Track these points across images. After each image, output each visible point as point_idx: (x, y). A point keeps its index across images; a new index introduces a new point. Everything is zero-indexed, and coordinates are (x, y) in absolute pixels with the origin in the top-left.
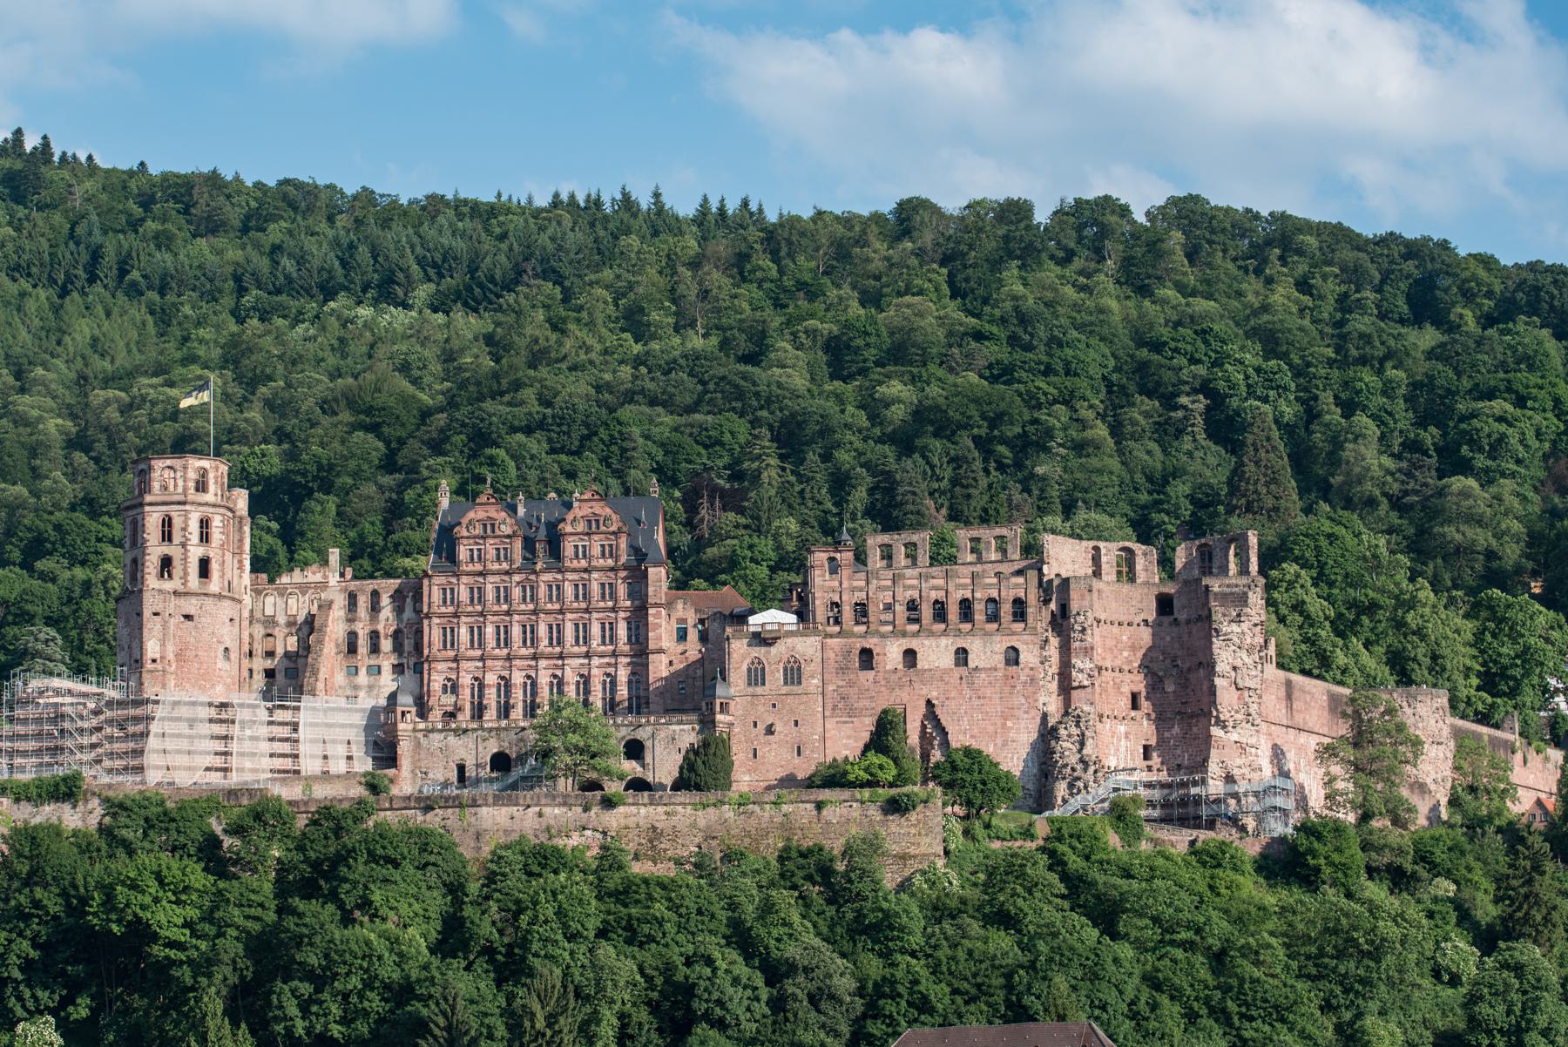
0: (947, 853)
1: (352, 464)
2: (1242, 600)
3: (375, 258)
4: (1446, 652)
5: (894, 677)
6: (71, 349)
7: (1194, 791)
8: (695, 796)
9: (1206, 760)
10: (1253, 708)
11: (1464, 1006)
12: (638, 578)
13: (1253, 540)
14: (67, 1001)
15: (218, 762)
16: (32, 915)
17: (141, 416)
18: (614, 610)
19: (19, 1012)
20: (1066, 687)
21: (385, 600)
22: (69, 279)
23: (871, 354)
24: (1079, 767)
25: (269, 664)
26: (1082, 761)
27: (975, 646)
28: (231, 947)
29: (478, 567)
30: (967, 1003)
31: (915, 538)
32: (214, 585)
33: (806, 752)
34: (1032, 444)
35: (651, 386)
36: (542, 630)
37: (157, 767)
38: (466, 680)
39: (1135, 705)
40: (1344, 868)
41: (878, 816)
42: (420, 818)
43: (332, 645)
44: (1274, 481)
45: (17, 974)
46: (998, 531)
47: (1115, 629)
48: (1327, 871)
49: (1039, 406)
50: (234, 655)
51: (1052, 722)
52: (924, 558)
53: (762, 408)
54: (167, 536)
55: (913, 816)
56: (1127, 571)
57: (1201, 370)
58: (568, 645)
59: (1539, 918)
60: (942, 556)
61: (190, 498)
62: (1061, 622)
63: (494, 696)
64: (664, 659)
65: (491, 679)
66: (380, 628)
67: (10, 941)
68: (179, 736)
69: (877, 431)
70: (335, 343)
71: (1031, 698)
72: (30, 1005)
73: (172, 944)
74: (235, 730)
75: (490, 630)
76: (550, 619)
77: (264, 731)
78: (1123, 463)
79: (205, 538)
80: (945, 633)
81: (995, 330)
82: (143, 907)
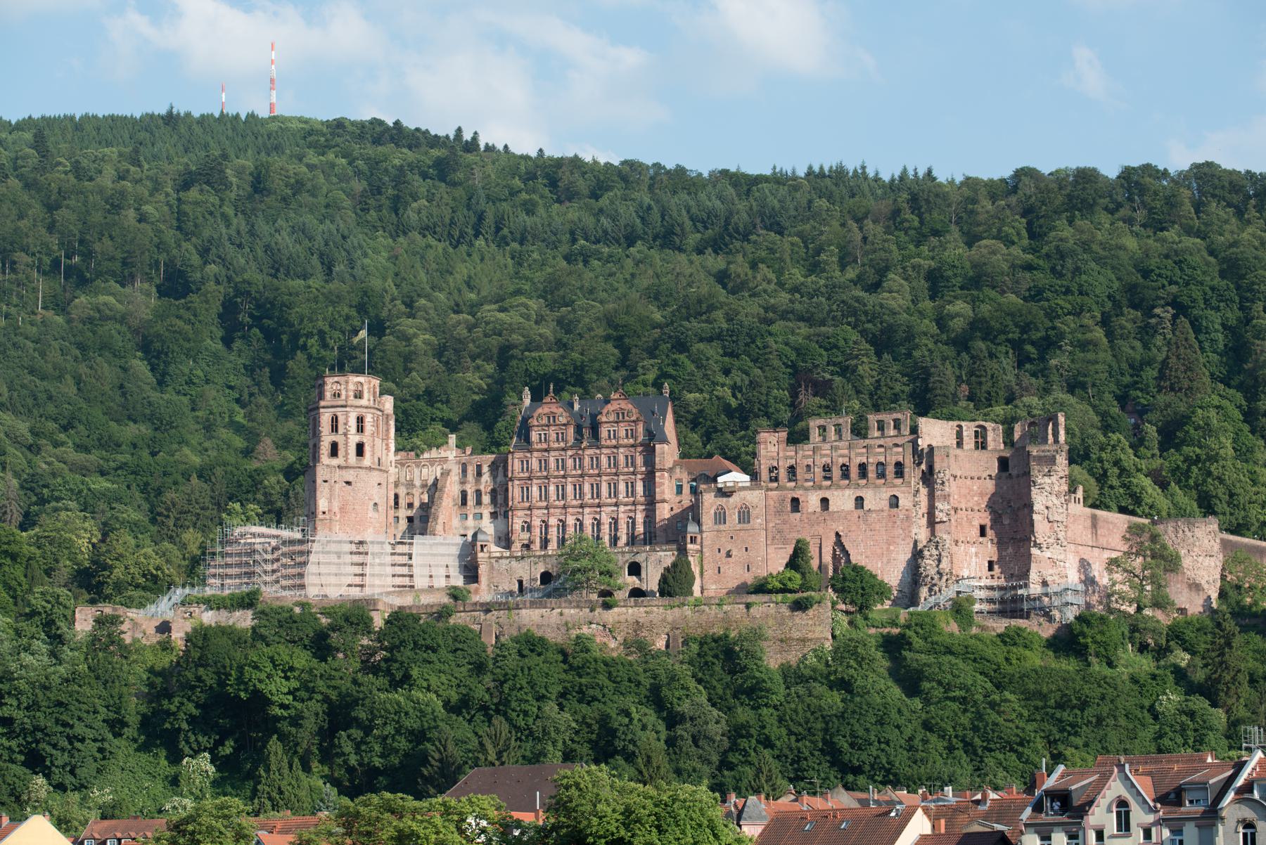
0: (834, 637)
1: (597, 365)
2: (1052, 461)
3: (663, 219)
4: (1238, 491)
5: (814, 517)
6: (452, 285)
7: (1020, 592)
8: (666, 600)
9: (1028, 571)
10: (1061, 535)
11: (1155, 739)
12: (649, 453)
13: (1061, 419)
14: (220, 742)
15: (358, 580)
16: (195, 687)
17: (478, 332)
18: (634, 473)
19: (187, 750)
20: (932, 523)
21: (485, 469)
22: (462, 236)
23: (958, 281)
24: (936, 577)
25: (410, 513)
26: (939, 573)
28: (315, 706)
29: (545, 446)
30: (798, 741)
31: (841, 421)
32: (367, 460)
33: (753, 569)
34: (1049, 344)
35: (797, 306)
36: (587, 488)
37: (315, 585)
38: (537, 522)
40: (1105, 645)
41: (787, 613)
42: (483, 617)
43: (450, 500)
44: (1189, 369)
45: (185, 726)
46: (895, 416)
47: (969, 482)
48: (1092, 648)
49: (1058, 317)
50: (381, 508)
51: (920, 546)
52: (847, 434)
53: (869, 321)
54: (335, 429)
55: (810, 612)
56: (981, 445)
57: (1174, 289)
58: (603, 498)
59: (1228, 678)
60: (859, 431)
61: (349, 403)
62: (928, 478)
63: (555, 533)
64: (667, 506)
65: (553, 521)
66: (482, 488)
67: (182, 704)
68: (329, 563)
69: (944, 337)
70: (628, 277)
71: (906, 530)
72: (195, 746)
73: (283, 706)
74: (369, 559)
75: (552, 488)
76: (592, 480)
77: (389, 559)
78: (1114, 356)
79: (360, 429)
80: (848, 486)
81: (1041, 262)
82: (260, 681)
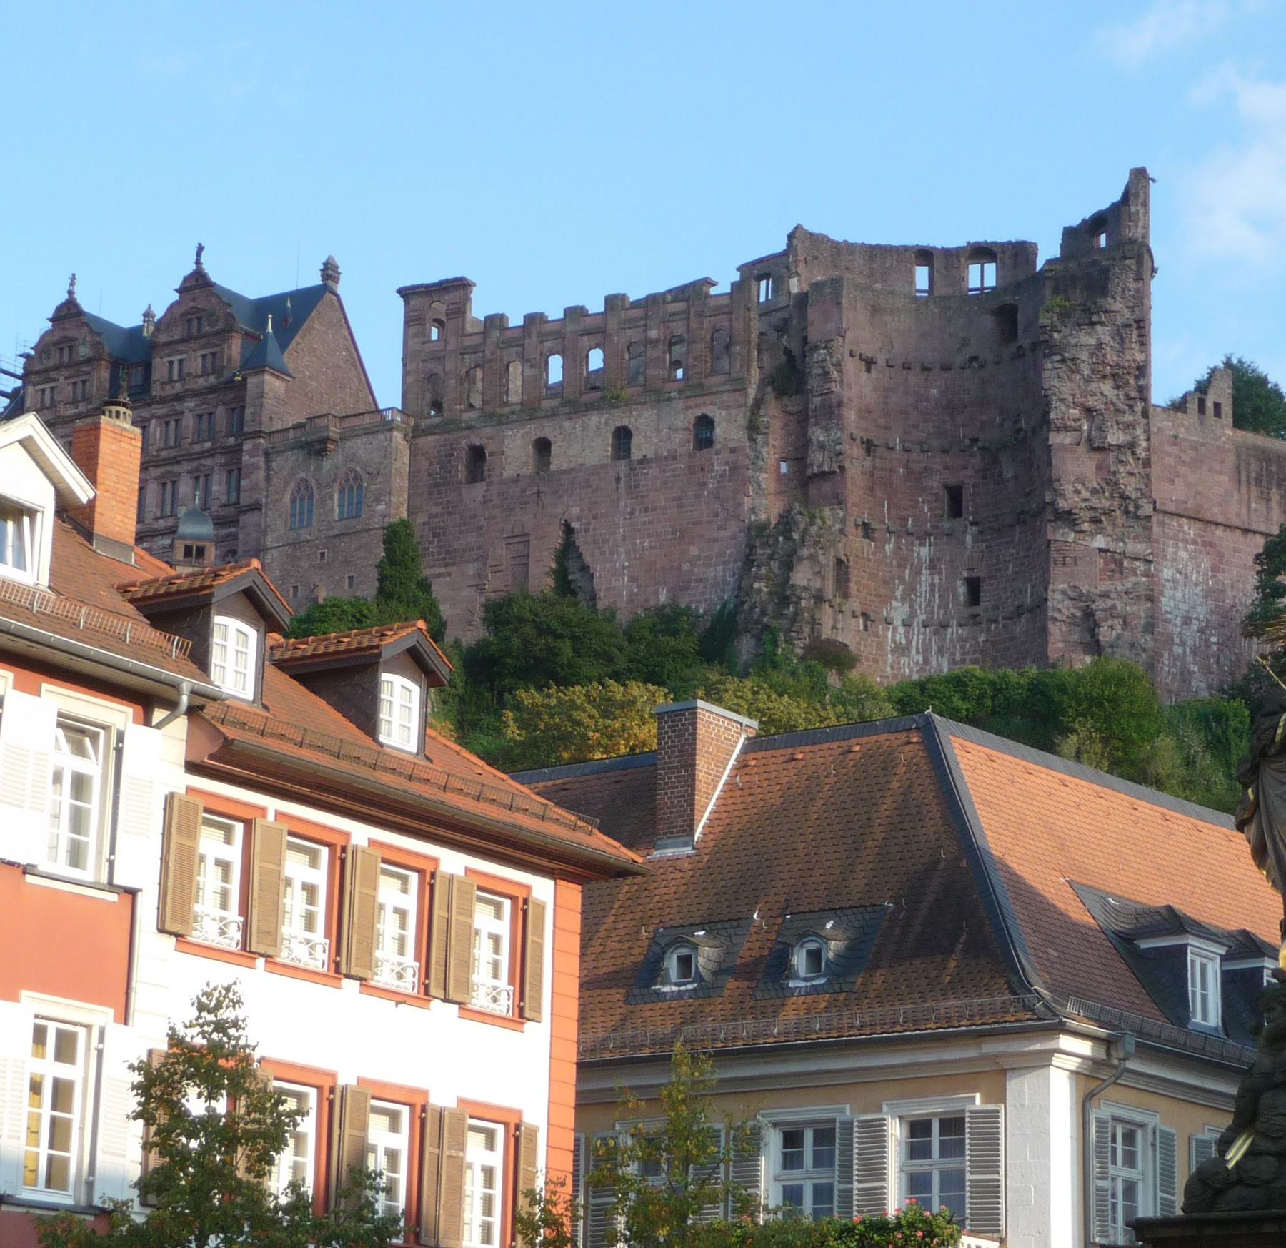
18: (210, 454)
27: (642, 422)
39: (956, 509)
47: (914, 379)
80: (590, 407)
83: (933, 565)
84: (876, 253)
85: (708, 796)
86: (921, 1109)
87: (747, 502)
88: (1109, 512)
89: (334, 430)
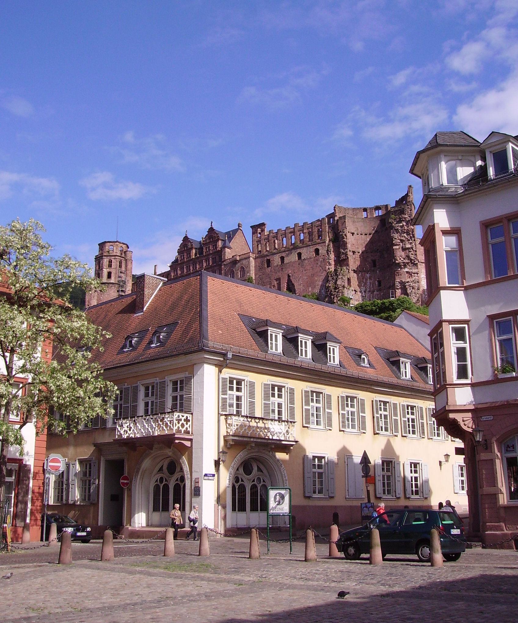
18: (215, 266)
32: (112, 280)
39: (375, 265)
47: (363, 236)
79: (110, 266)
83: (370, 278)
84: (354, 209)
85: (149, 299)
86: (174, 377)
87: (327, 267)
88: (408, 263)
89: (238, 258)
